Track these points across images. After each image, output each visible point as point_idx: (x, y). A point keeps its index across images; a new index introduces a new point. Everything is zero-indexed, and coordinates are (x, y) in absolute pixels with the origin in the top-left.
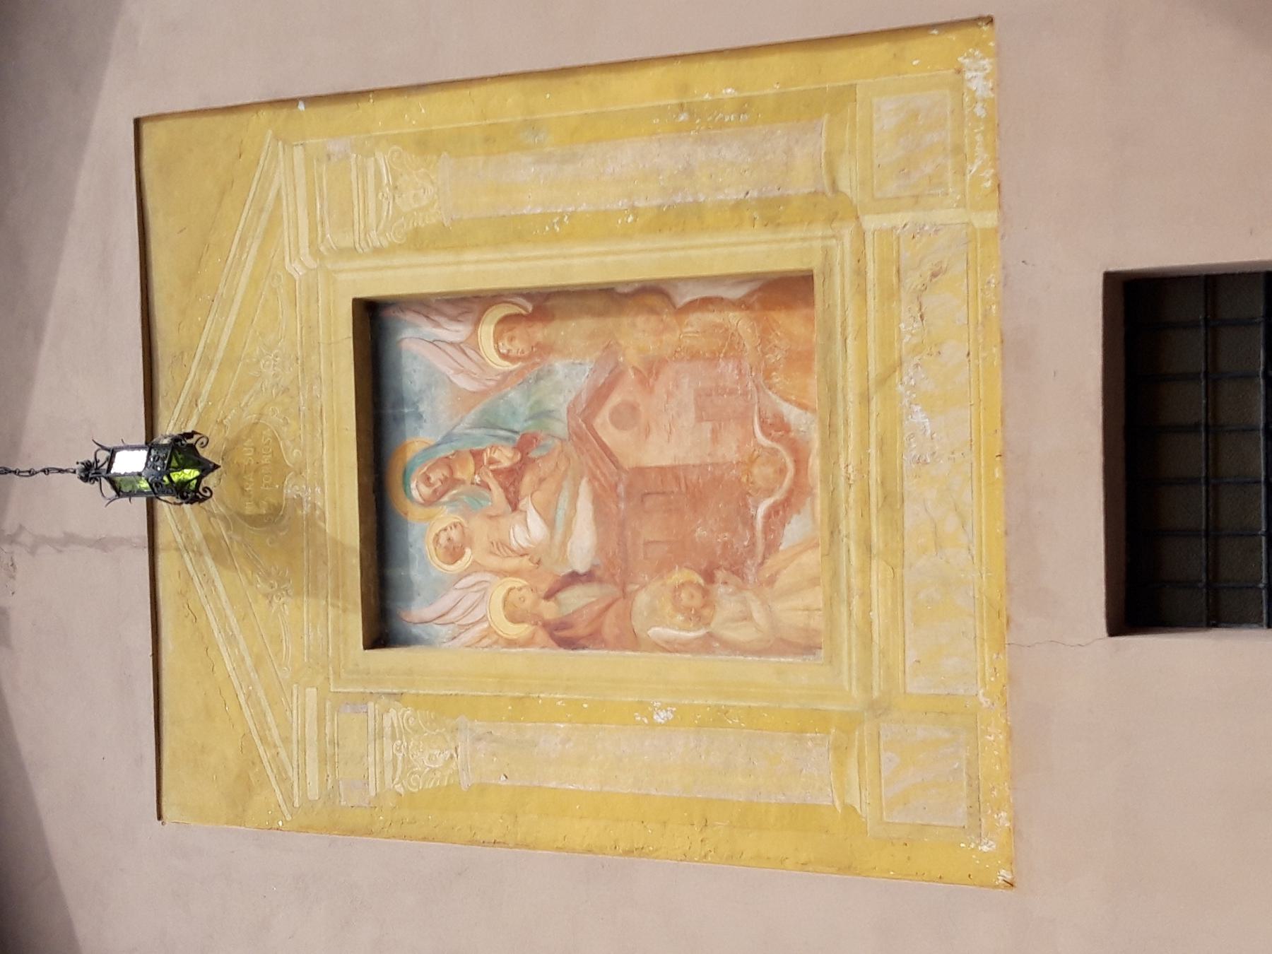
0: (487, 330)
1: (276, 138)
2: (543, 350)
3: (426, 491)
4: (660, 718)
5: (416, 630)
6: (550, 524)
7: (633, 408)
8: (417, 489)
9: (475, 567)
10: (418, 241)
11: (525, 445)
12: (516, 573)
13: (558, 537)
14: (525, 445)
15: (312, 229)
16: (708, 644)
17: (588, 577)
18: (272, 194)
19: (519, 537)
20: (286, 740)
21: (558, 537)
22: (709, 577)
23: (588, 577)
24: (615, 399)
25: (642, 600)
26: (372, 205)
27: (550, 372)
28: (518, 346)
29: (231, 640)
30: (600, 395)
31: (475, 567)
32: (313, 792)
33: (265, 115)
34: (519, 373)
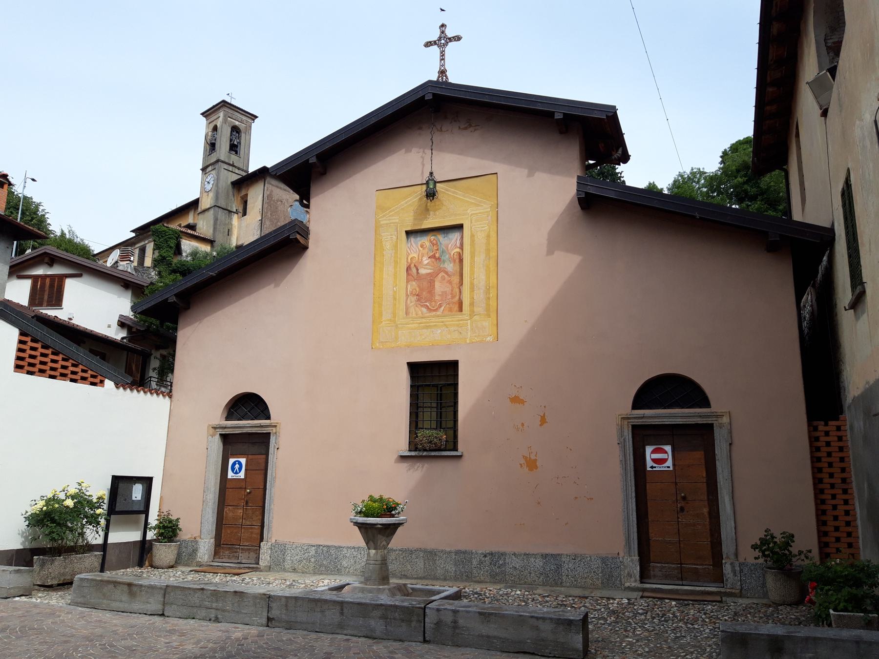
0: (458, 250)
1: (492, 205)
2: (455, 261)
3: (432, 240)
4: (395, 288)
5: (409, 240)
6: (426, 265)
7: (444, 279)
8: (432, 238)
9: (419, 250)
10: (472, 236)
11: (439, 259)
12: (418, 259)
13: (424, 266)
14: (439, 259)
15: (476, 214)
16: (407, 295)
17: (418, 273)
18: (482, 205)
19: (424, 259)
20: (389, 216)
21: (424, 266)
22: (417, 295)
23: (418, 273)
24: (446, 276)
25: (414, 283)
26: (479, 226)
27: (451, 263)
28: (455, 256)
29: (406, 203)
30: (446, 273)
31: (419, 250)
32: (382, 223)
33: (496, 202)
34: (451, 257)
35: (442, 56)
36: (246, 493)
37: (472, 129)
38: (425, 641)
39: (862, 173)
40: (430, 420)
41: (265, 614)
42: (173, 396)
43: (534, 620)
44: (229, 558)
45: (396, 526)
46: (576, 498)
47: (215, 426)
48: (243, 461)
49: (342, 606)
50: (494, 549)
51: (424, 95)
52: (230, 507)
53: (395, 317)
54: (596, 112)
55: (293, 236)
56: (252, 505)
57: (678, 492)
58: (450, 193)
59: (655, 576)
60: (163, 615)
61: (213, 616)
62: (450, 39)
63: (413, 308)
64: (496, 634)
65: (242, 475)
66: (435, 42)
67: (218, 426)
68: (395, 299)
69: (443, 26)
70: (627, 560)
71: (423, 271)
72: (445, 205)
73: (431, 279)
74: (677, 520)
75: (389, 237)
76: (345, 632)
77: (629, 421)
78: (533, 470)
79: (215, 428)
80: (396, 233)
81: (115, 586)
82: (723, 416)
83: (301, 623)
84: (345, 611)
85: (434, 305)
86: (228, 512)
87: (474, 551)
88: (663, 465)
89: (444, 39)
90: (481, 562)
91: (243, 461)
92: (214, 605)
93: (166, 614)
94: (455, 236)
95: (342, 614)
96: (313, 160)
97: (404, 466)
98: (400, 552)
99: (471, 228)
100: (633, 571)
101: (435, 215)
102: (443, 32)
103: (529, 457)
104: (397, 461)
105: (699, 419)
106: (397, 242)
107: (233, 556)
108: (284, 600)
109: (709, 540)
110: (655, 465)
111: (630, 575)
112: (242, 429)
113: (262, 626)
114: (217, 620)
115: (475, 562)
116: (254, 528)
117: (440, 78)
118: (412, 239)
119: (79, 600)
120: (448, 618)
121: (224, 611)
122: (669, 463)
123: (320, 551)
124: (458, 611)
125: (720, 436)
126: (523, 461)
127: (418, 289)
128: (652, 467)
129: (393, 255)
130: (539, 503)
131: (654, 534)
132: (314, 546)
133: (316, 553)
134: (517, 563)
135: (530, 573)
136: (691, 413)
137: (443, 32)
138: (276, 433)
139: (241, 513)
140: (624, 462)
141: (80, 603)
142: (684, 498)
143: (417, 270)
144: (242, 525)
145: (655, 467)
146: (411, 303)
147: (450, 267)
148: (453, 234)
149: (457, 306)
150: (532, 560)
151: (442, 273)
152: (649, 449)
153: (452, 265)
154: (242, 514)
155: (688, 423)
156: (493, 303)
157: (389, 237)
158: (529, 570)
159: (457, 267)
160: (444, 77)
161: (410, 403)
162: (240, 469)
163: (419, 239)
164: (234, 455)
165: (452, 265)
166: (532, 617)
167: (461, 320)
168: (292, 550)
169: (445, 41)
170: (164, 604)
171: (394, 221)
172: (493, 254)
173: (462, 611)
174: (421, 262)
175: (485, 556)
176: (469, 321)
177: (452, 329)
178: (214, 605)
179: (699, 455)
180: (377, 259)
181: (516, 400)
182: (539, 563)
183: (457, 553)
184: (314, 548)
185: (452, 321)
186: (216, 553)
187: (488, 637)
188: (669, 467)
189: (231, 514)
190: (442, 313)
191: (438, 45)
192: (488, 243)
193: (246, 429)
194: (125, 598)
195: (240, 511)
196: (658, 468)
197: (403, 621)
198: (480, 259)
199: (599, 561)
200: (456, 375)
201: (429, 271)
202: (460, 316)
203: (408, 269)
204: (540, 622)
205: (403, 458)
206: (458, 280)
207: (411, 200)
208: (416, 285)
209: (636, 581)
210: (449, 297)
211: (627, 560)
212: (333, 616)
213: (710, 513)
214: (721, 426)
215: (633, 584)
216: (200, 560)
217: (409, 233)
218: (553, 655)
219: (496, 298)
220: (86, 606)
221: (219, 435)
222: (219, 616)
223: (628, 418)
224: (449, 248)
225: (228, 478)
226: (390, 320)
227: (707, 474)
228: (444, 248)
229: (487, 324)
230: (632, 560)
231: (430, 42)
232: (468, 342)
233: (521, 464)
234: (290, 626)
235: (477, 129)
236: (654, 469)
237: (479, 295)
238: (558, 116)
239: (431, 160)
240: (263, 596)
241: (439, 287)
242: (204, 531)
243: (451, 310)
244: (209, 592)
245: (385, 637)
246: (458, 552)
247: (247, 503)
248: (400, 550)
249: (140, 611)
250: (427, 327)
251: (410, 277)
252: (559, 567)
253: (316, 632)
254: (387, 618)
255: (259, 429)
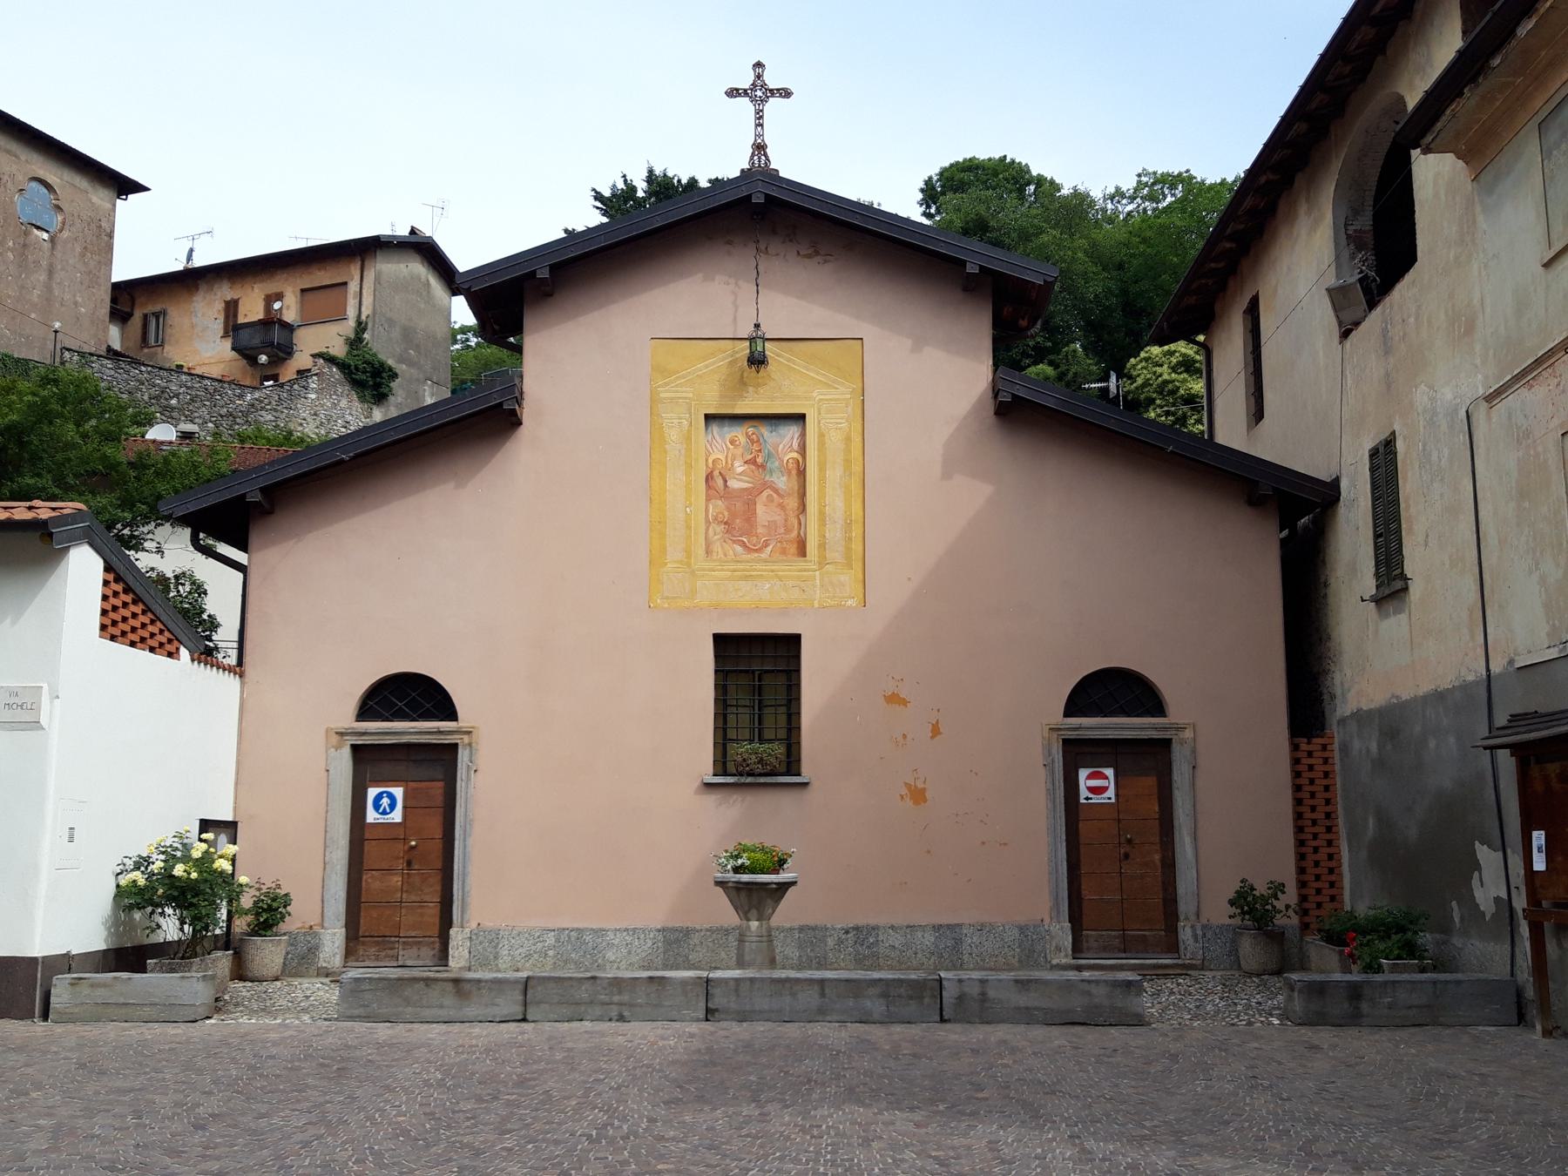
0: (795, 455)
1: (854, 389)
2: (789, 473)
3: (750, 434)
4: (688, 510)
5: (710, 428)
6: (740, 474)
7: (773, 501)
8: (751, 430)
9: (728, 449)
10: (821, 435)
11: (763, 467)
12: (726, 462)
13: (737, 477)
14: (763, 467)
15: (827, 400)
16: (708, 522)
17: (726, 486)
19: (737, 464)
20: (676, 386)
21: (737, 477)
22: (725, 523)
23: (726, 486)
24: (775, 495)
25: (720, 503)
26: (832, 421)
27: (783, 476)
28: (790, 466)
29: (707, 367)
30: (776, 491)
31: (728, 449)
32: (662, 395)
33: (860, 385)
34: (783, 466)
35: (759, 119)
36: (406, 847)
37: (819, 259)
38: (943, 1020)
39: (1424, 450)
40: (735, 726)
41: (702, 1005)
42: (247, 673)
43: (1086, 984)
44: (377, 959)
45: (784, 887)
46: (983, 843)
47: (344, 730)
48: (398, 792)
49: (823, 990)
50: (861, 922)
51: (750, 195)
52: (374, 872)
53: (689, 557)
54: (1028, 272)
55: (509, 405)
56: (419, 868)
57: (1121, 833)
58: (781, 360)
59: (1089, 949)
60: (524, 1020)
61: (614, 1014)
62: (771, 91)
63: (718, 544)
64: (1036, 1004)
65: (397, 816)
66: (745, 90)
67: (349, 731)
68: (689, 527)
69: (759, 65)
70: (1055, 928)
71: (734, 484)
72: (774, 380)
73: (749, 499)
74: (1118, 871)
75: (676, 421)
76: (829, 1018)
77: (1060, 733)
78: (920, 804)
79: (341, 734)
80: (688, 415)
81: (427, 985)
82: (1185, 728)
83: (761, 1012)
84: (827, 991)
85: (754, 542)
86: (369, 880)
87: (829, 926)
88: (1102, 796)
89: (761, 90)
90: (840, 942)
91: (398, 792)
92: (616, 999)
93: (528, 1017)
94: (789, 431)
95: (823, 995)
96: (543, 274)
97: (712, 799)
98: (708, 933)
99: (819, 423)
100: (1063, 944)
101: (756, 393)
102: (759, 77)
103: (913, 784)
104: (697, 792)
105: (1154, 733)
106: (689, 431)
107: (387, 956)
108: (732, 983)
109: (1161, 896)
110: (1091, 796)
111: (1058, 949)
112: (397, 737)
113: (698, 1020)
114: (621, 1018)
115: (831, 942)
116: (427, 906)
117: (756, 158)
118: (715, 428)
119: (356, 1012)
120: (974, 991)
121: (632, 1005)
122: (1111, 793)
123: (564, 937)
124: (987, 980)
125: (1179, 755)
126: (904, 791)
127: (726, 514)
128: (1087, 799)
129: (683, 452)
130: (929, 852)
131: (1088, 894)
132: (554, 930)
133: (558, 940)
134: (896, 940)
135: (916, 954)
136: (1144, 724)
137: (759, 77)
138: (470, 745)
139: (398, 881)
140: (1051, 793)
141: (359, 1017)
142: (1129, 841)
143: (725, 481)
144: (401, 902)
145: (1091, 799)
146: (715, 534)
147: (782, 482)
148: (786, 428)
149: (795, 546)
150: (919, 934)
151: (768, 490)
152: (1083, 774)
153: (784, 479)
154: (400, 883)
155: (1138, 737)
156: (856, 546)
157: (676, 421)
158: (914, 949)
159: (794, 484)
160: (763, 158)
161: (715, 699)
162: (393, 806)
163: (726, 429)
164: (377, 782)
165: (784, 479)
166: (1083, 981)
167: (805, 571)
168: (511, 939)
169: (763, 93)
170: (525, 1004)
171: (684, 395)
172: (857, 468)
173: (993, 980)
174: (731, 469)
175: (847, 932)
176: (817, 573)
177: (790, 583)
178: (616, 999)
179: (1150, 782)
180: (653, 456)
181: (893, 699)
182: (929, 939)
183: (802, 929)
184: (553, 933)
185: (789, 570)
186: (349, 953)
187: (1027, 1008)
188: (1110, 798)
189: (377, 885)
190: (770, 556)
191: (751, 98)
192: (848, 451)
193: (408, 737)
194: (449, 1000)
195: (396, 879)
196: (1096, 799)
197: (911, 998)
198: (835, 474)
199: (1016, 931)
200: (797, 657)
201: (745, 485)
202: (800, 564)
203: (709, 478)
204: (1093, 985)
205: (709, 786)
206: (796, 504)
207: (714, 363)
208: (723, 506)
209: (1066, 956)
210: (782, 530)
211: (1055, 928)
212: (809, 998)
213: (1163, 860)
214: (1182, 742)
215: (1064, 961)
216: (324, 965)
217: (709, 418)
218: (1108, 1023)
219: (861, 539)
220: (372, 1020)
221: (349, 746)
222: (626, 1014)
223: (1060, 729)
224: (780, 449)
225: (368, 821)
226: (681, 562)
227: (1160, 809)
228: (771, 449)
229: (848, 579)
230: (1062, 928)
231: (737, 90)
232: (816, 605)
233: (902, 797)
234: (743, 1017)
235: (829, 261)
236: (1090, 801)
237: (834, 533)
238: (971, 269)
239: (757, 303)
240: (698, 981)
241: (764, 513)
242: (329, 913)
243: (784, 552)
244: (607, 981)
245: (887, 1020)
246: (801, 929)
247: (409, 863)
248: (707, 930)
249: (479, 1019)
250: (746, 578)
251: (712, 492)
252: (958, 942)
253: (784, 1021)
254: (889, 996)
255: (375, 738)
